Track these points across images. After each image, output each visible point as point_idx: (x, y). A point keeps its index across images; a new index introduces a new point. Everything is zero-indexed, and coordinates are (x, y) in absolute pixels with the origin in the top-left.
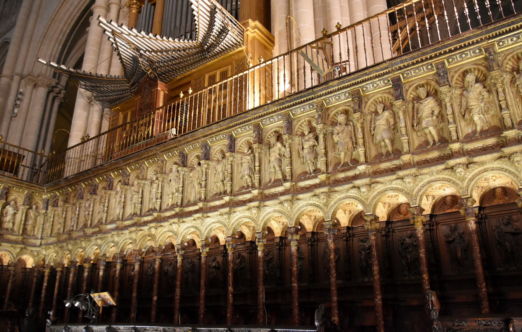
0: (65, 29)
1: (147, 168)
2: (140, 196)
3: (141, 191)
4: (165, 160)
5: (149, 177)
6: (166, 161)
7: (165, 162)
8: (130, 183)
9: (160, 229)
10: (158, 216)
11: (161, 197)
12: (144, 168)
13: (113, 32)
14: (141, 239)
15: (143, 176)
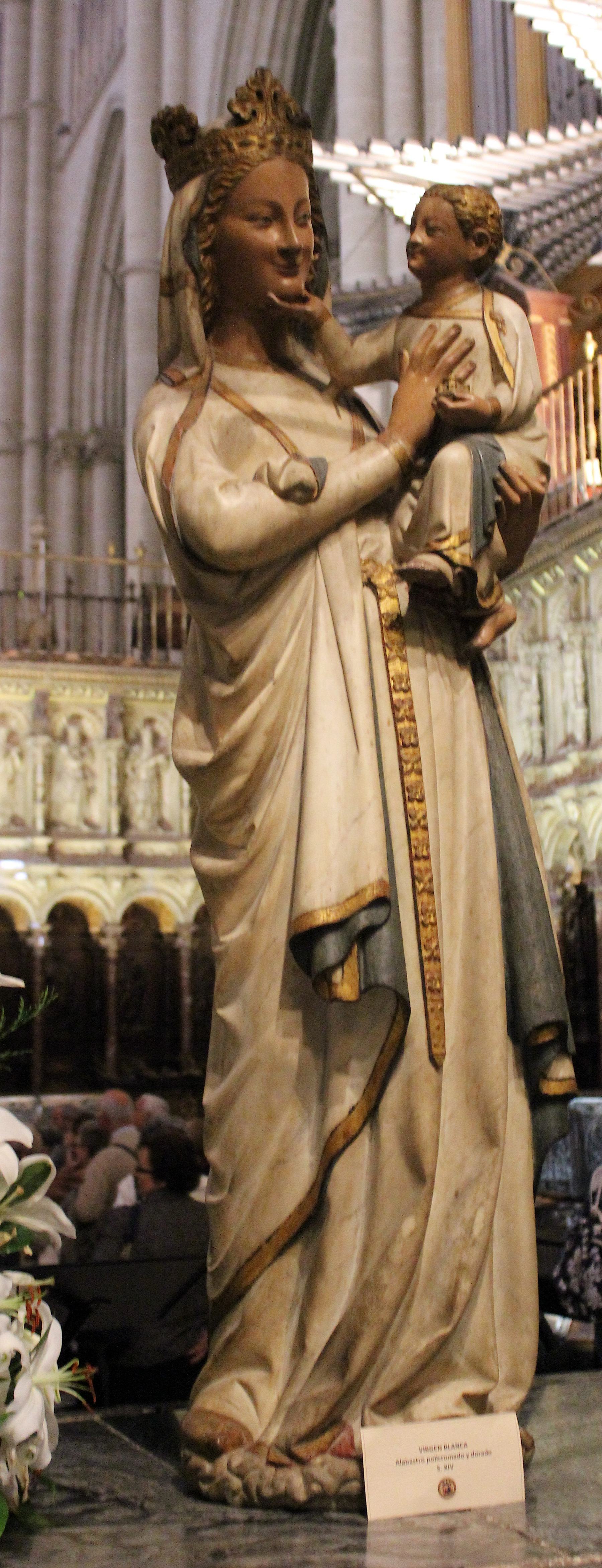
0: (283, 28)
1: (544, 601)
2: (536, 697)
3: (535, 681)
4: (580, 571)
5: (552, 631)
6: (587, 577)
7: (582, 580)
8: (510, 651)
9: (591, 805)
10: (584, 762)
11: (586, 700)
12: (532, 603)
13: (352, 170)
14: (552, 836)
15: (534, 631)
